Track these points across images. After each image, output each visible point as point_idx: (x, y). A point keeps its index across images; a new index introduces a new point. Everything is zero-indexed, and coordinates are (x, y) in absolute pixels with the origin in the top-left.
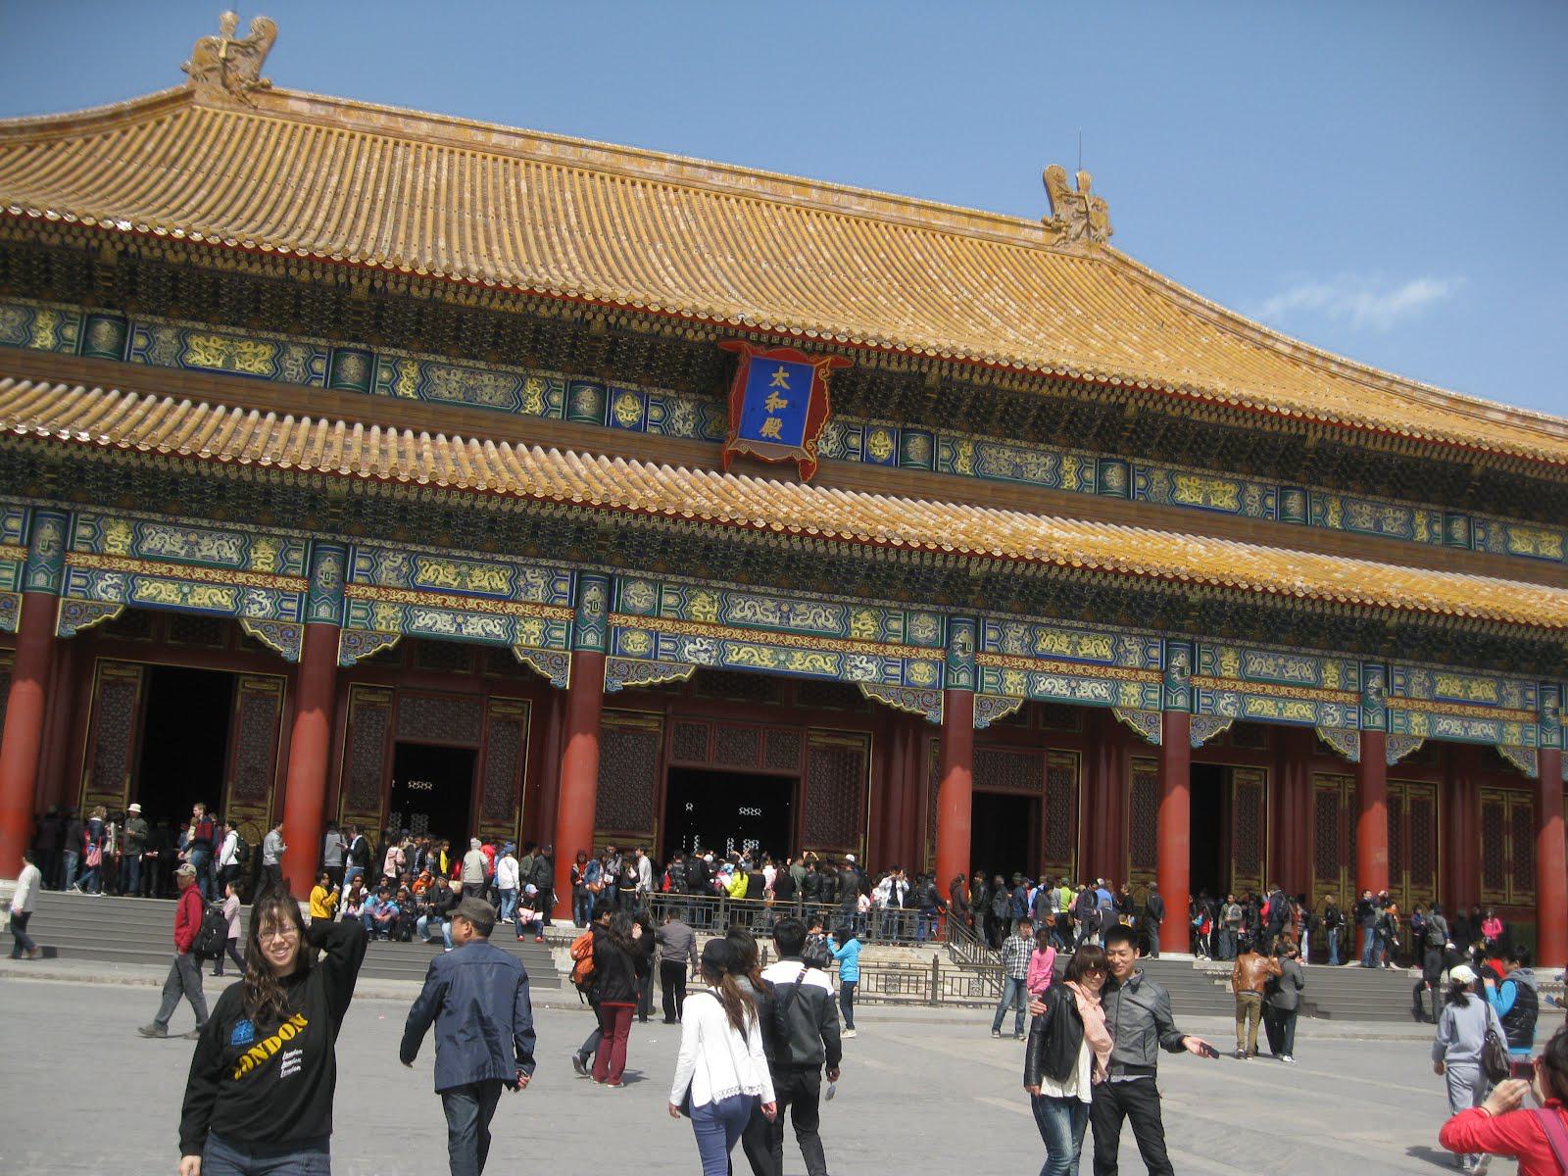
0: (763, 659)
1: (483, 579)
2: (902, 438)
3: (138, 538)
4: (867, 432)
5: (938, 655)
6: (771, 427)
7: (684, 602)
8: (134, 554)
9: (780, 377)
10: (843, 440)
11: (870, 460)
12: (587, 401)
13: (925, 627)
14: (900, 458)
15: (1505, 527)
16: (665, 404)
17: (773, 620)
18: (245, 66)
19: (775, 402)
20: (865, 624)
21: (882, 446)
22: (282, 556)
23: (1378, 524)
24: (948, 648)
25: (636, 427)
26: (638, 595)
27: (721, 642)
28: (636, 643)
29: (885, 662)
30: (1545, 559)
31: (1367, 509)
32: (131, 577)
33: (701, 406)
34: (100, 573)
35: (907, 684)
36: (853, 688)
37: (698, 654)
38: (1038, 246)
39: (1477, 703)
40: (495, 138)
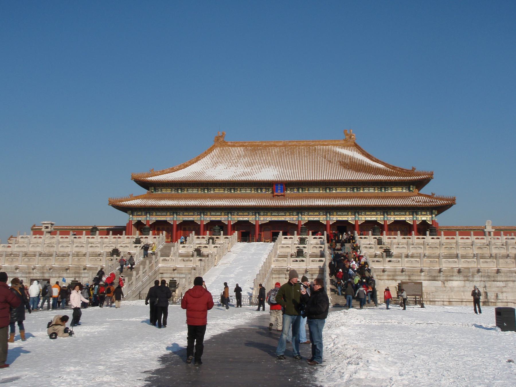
6: (279, 191)
13: (295, 213)
20: (288, 214)
40: (257, 143)
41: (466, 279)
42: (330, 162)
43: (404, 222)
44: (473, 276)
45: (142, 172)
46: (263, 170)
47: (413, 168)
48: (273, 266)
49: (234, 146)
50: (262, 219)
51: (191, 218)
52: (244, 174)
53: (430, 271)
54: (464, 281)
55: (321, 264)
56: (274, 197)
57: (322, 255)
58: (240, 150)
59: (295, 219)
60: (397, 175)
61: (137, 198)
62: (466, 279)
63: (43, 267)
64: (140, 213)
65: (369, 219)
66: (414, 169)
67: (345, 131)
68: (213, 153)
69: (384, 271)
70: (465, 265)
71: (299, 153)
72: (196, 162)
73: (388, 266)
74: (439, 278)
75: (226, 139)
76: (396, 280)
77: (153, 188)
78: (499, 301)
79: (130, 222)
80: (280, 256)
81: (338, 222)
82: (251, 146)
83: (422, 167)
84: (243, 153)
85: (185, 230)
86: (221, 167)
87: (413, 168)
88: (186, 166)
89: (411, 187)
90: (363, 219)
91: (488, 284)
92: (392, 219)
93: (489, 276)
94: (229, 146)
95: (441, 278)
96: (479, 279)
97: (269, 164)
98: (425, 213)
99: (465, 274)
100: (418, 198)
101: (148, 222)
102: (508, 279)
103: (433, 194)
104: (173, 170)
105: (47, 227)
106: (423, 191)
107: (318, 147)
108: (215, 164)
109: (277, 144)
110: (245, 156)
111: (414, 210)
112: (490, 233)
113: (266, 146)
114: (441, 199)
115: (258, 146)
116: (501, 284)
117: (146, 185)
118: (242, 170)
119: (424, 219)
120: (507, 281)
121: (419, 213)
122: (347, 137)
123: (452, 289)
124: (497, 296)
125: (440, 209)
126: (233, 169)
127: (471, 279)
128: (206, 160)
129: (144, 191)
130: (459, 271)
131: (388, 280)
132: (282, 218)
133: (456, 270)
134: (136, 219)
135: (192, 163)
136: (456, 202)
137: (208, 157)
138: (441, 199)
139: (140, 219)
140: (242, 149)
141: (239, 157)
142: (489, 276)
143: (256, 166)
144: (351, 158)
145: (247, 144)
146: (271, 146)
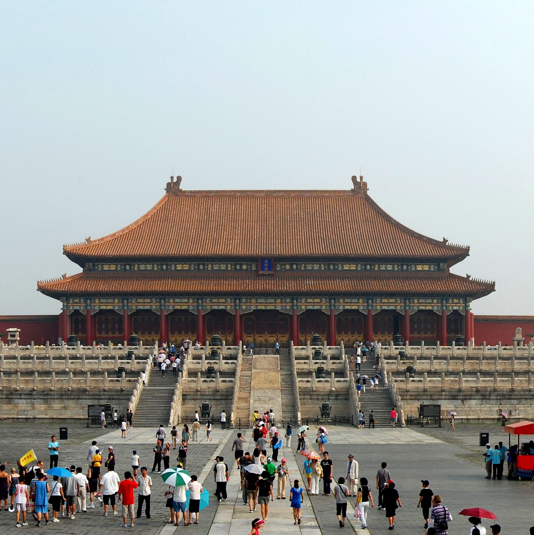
0: (263, 308)
1: (221, 300)
2: (291, 265)
3: (174, 300)
4: (286, 264)
5: (291, 304)
7: (251, 300)
8: (174, 302)
9: (266, 261)
10: (281, 267)
11: (286, 270)
12: (238, 267)
13: (288, 300)
14: (291, 269)
15: (415, 265)
16: (251, 265)
17: (264, 302)
18: (176, 187)
19: (266, 265)
20: (279, 301)
21: (288, 267)
22: (193, 300)
23: (386, 268)
24: (292, 303)
25: (246, 270)
26: (244, 300)
27: (257, 306)
28: (244, 307)
29: (282, 306)
30: (425, 270)
31: (384, 266)
32: (173, 306)
33: (256, 264)
34: (169, 306)
35: (286, 309)
36: (278, 310)
37: (253, 308)
38: (350, 196)
39: (391, 303)
41: (483, 397)
47: (444, 239)
54: (482, 399)
59: (288, 307)
62: (483, 397)
64: (77, 300)
67: (354, 178)
73: (412, 385)
74: (458, 397)
76: (418, 400)
77: (91, 264)
78: (512, 417)
83: (456, 240)
87: (444, 239)
89: (441, 265)
91: (503, 402)
95: (461, 397)
96: (495, 398)
98: (457, 301)
99: (482, 393)
102: (522, 397)
105: (14, 336)
111: (444, 296)
116: (515, 402)
120: (520, 399)
121: (450, 300)
124: (510, 414)
127: (487, 397)
131: (411, 399)
139: (78, 308)
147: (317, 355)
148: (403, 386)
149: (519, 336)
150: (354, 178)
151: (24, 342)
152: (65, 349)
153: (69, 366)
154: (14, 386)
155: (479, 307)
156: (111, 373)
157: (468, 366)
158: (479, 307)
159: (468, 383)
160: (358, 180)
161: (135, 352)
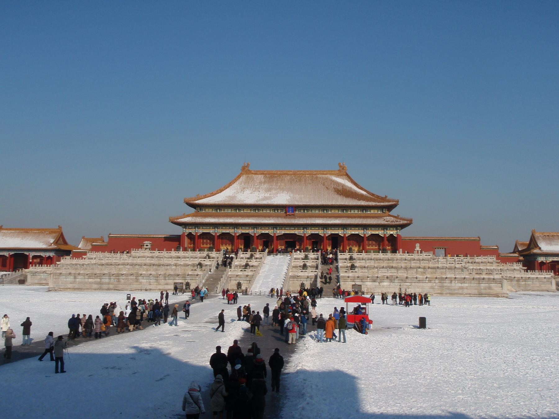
13: (302, 228)
42: (327, 188)
43: (378, 235)
44: (394, 280)
45: (189, 196)
46: (278, 195)
48: (290, 274)
49: (256, 174)
50: (278, 232)
51: (227, 231)
52: (265, 198)
53: (372, 277)
55: (316, 273)
56: (287, 216)
57: (317, 267)
58: (261, 177)
60: (374, 201)
61: (188, 216)
63: (165, 274)
65: (354, 233)
66: (386, 197)
67: (339, 164)
68: (241, 180)
69: (348, 277)
70: (391, 274)
71: (305, 180)
72: (228, 187)
73: (351, 274)
75: (250, 168)
79: (184, 233)
80: (294, 267)
81: (332, 234)
82: (269, 174)
84: (263, 180)
85: (222, 239)
86: (247, 192)
88: (221, 191)
90: (350, 233)
92: (370, 233)
93: (402, 280)
94: (253, 174)
97: (283, 190)
100: (388, 218)
101: (196, 233)
103: (398, 216)
104: (212, 194)
106: (391, 213)
107: (319, 176)
108: (243, 189)
109: (288, 173)
110: (265, 182)
111: (384, 227)
112: (418, 251)
113: (280, 174)
114: (404, 220)
115: (274, 174)
117: (194, 206)
118: (263, 195)
119: (391, 233)
122: (341, 169)
123: (383, 286)
125: (403, 226)
126: (256, 193)
128: (236, 185)
129: (193, 210)
130: (387, 278)
132: (292, 232)
133: (386, 277)
134: (188, 231)
135: (226, 188)
136: (413, 222)
137: (237, 182)
138: (404, 220)
140: (263, 176)
141: (260, 183)
142: (402, 280)
143: (273, 192)
144: (343, 186)
145: (266, 172)
146: (284, 174)
147: (306, 257)
148: (347, 275)
149: (418, 248)
150: (339, 164)
151: (153, 248)
152: (173, 253)
153: (173, 262)
154: (140, 272)
155: (404, 233)
156: (193, 265)
157: (385, 264)
158: (404, 233)
159: (381, 273)
160: (341, 164)
161: (210, 255)
